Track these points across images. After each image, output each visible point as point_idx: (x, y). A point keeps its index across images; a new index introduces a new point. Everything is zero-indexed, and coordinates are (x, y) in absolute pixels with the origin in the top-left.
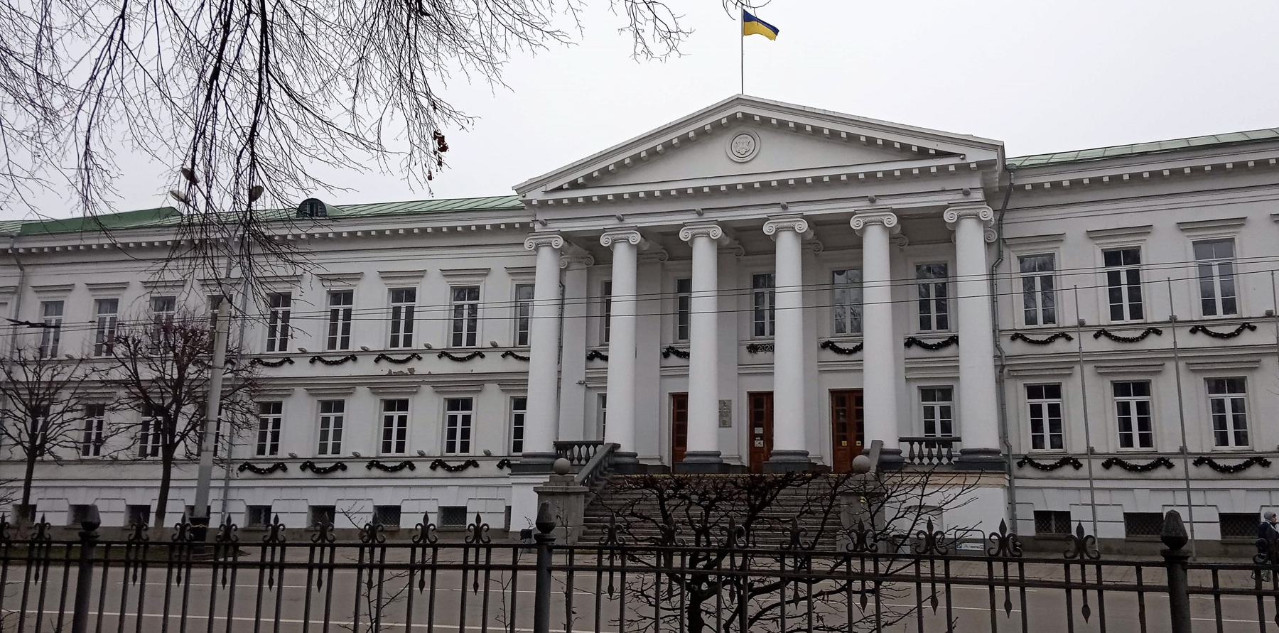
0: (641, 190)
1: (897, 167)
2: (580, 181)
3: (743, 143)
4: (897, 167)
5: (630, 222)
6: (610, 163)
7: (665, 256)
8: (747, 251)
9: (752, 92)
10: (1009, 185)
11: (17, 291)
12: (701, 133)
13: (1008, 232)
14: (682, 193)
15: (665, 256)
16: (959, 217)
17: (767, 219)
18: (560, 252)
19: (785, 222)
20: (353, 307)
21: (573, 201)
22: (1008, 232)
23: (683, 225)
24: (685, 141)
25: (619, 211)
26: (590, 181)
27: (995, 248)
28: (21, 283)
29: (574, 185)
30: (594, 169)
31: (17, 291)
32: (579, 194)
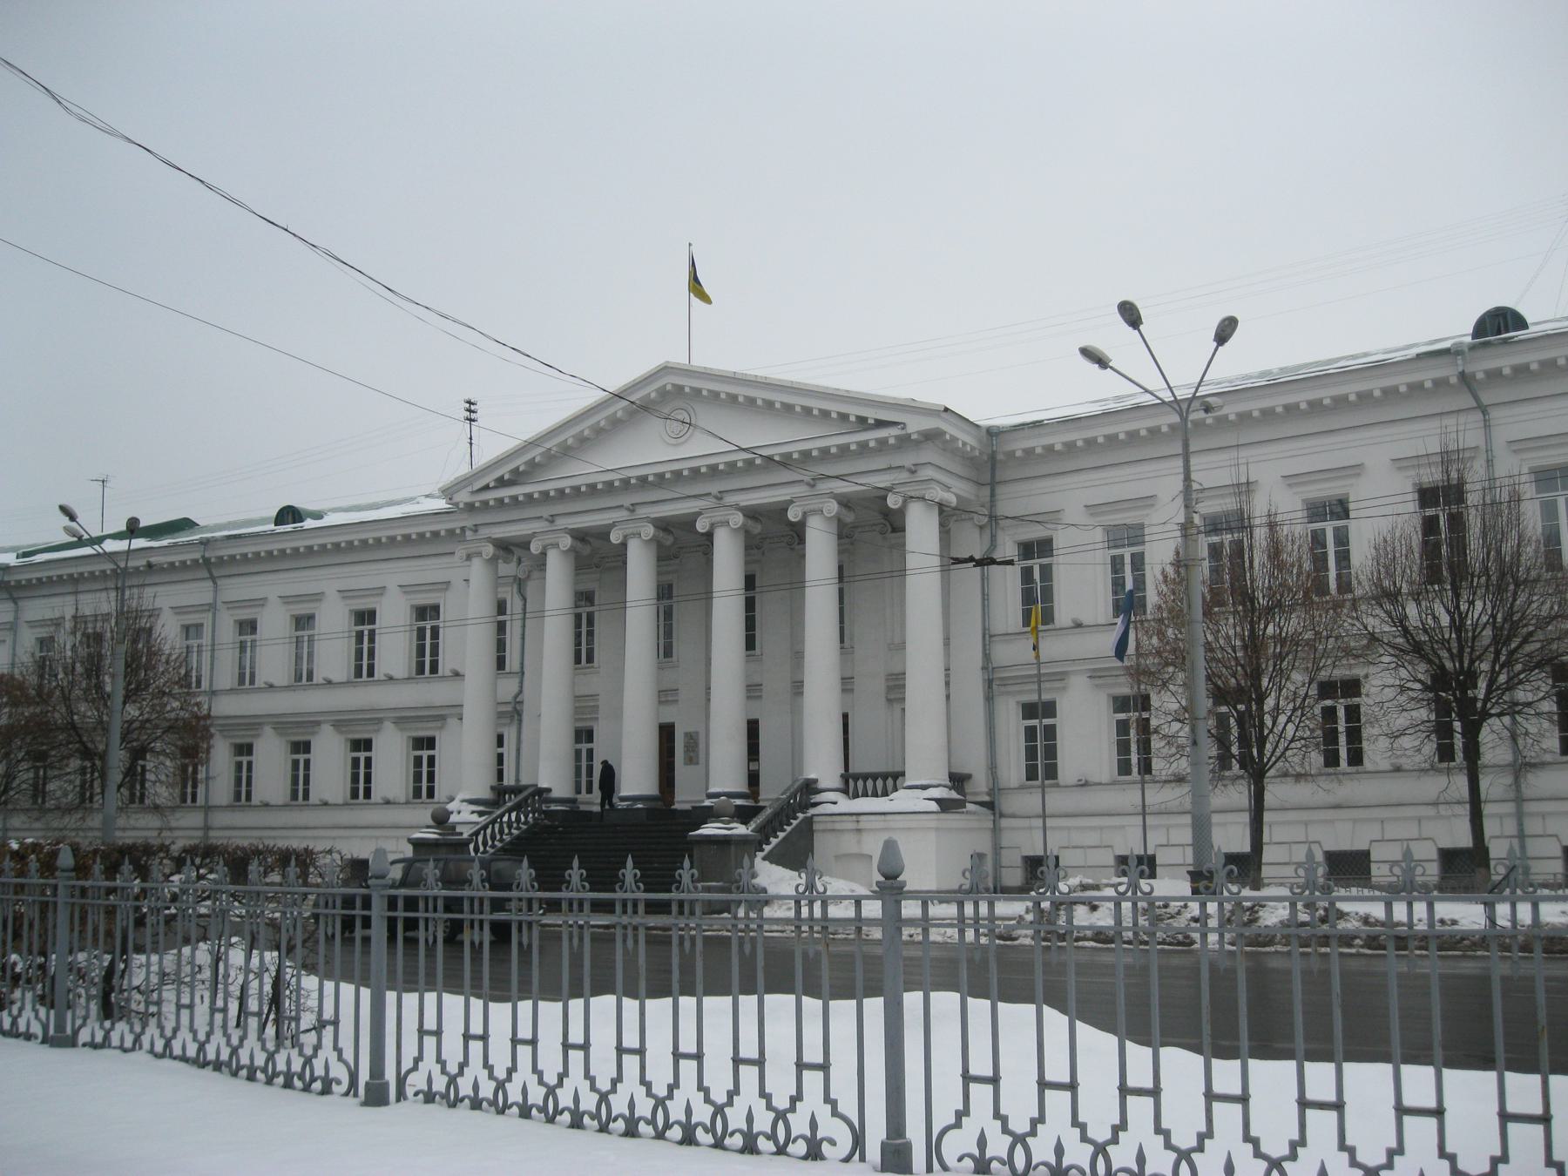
2: (506, 477)
4: (853, 439)
5: (562, 523)
7: (597, 559)
8: (682, 548)
9: (701, 361)
11: (13, 627)
15: (597, 559)
16: (805, 514)
17: (699, 514)
20: (376, 626)
21: (500, 501)
25: (546, 511)
27: (988, 531)
28: (16, 618)
30: (519, 462)
31: (13, 627)
32: (506, 493)
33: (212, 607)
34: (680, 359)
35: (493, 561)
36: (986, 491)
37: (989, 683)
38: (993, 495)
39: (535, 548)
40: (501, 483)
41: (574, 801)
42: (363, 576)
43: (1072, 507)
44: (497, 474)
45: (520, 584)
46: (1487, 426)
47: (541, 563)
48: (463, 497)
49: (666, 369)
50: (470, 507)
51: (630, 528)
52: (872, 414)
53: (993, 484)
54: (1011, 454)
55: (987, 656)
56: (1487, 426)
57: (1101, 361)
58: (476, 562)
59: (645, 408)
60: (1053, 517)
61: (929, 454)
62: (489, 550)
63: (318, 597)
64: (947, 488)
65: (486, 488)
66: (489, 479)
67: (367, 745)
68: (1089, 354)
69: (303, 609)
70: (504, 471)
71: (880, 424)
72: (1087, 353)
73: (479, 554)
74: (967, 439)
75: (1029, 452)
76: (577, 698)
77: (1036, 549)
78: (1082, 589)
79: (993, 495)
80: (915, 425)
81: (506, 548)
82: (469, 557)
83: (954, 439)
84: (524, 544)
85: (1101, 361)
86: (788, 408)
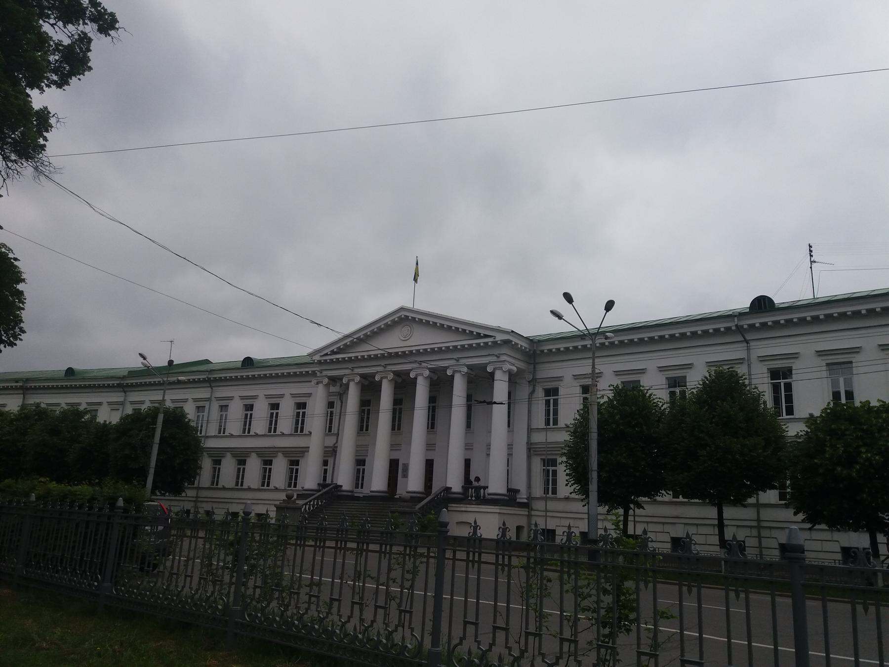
0: (359, 355)
3: (406, 330)
5: (357, 371)
10: (535, 352)
18: (327, 385)
23: (377, 372)
25: (350, 366)
26: (340, 351)
29: (333, 353)
30: (341, 344)
33: (209, 400)
35: (327, 385)
36: (532, 366)
37: (529, 449)
38: (535, 368)
39: (345, 381)
40: (333, 353)
41: (352, 492)
42: (275, 389)
43: (568, 375)
44: (331, 349)
47: (347, 385)
48: (317, 358)
49: (402, 309)
50: (319, 362)
54: (542, 351)
55: (529, 437)
57: (559, 317)
58: (321, 386)
60: (560, 379)
62: (326, 381)
63: (255, 397)
64: (513, 365)
65: (326, 354)
66: (328, 351)
68: (553, 313)
70: (334, 348)
72: (553, 313)
73: (322, 382)
75: (550, 350)
76: (357, 446)
77: (552, 392)
78: (569, 410)
79: (535, 368)
80: (500, 337)
81: (333, 380)
82: (318, 383)
83: (516, 344)
84: (340, 378)
85: (559, 317)
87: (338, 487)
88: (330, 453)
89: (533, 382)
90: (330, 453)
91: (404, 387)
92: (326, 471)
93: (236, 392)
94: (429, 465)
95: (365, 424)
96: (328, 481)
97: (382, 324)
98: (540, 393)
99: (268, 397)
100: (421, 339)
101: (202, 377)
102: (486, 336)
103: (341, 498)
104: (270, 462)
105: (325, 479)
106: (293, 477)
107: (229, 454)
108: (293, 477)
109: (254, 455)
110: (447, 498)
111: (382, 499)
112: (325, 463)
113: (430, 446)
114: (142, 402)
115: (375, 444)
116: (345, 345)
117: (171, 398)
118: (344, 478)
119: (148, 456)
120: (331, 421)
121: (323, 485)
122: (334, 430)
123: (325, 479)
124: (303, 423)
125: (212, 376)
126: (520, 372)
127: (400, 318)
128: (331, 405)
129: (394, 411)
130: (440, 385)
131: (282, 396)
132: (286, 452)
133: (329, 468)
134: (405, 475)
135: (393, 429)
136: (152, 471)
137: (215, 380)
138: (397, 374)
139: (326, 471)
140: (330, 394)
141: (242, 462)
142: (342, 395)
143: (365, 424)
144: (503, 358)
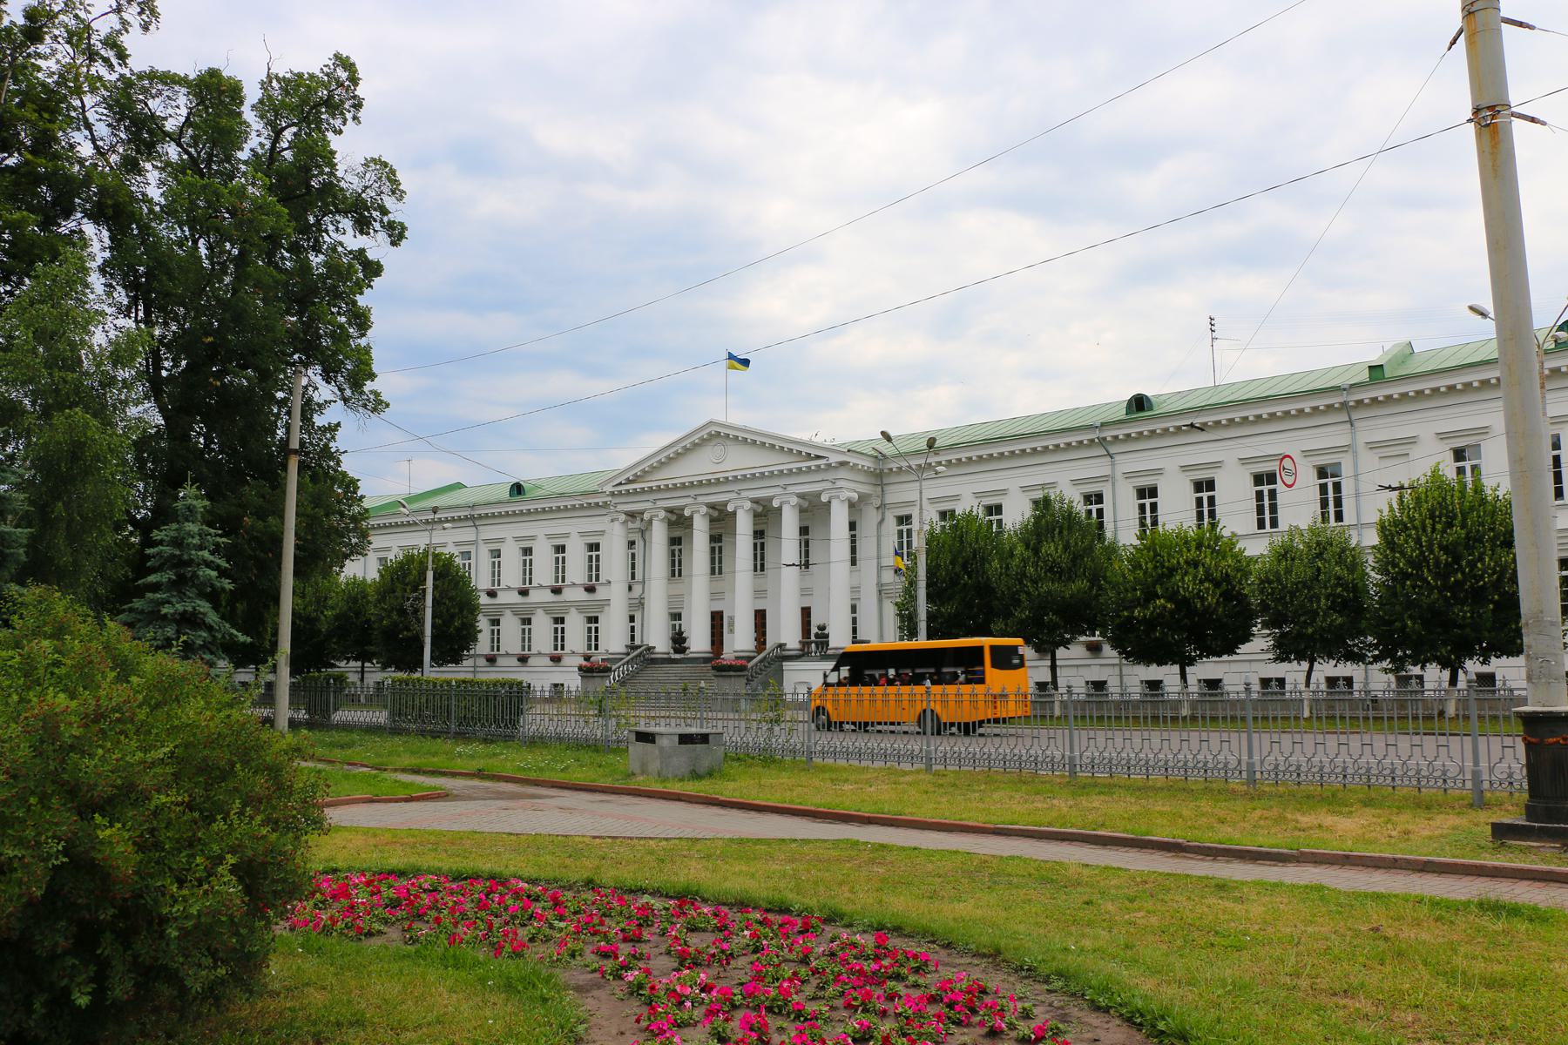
1: (804, 465)
4: (804, 465)
5: (660, 504)
6: (645, 466)
7: (679, 524)
12: (695, 446)
13: (889, 499)
14: (675, 487)
19: (739, 503)
22: (889, 499)
24: (686, 450)
25: (652, 497)
30: (637, 470)
32: (630, 487)
34: (721, 418)
35: (625, 522)
39: (646, 516)
40: (629, 481)
45: (643, 532)
46: (1113, 465)
47: (650, 522)
48: (608, 488)
50: (612, 494)
51: (695, 508)
52: (814, 452)
53: (882, 485)
55: (879, 576)
56: (1113, 465)
59: (703, 442)
61: (842, 473)
62: (623, 517)
66: (622, 479)
67: (562, 620)
69: (526, 544)
70: (630, 475)
71: (818, 457)
74: (867, 463)
76: (670, 596)
81: (632, 515)
84: (642, 513)
86: (773, 446)
87: (650, 649)
88: (636, 609)
89: (882, 507)
90: (636, 609)
91: (721, 520)
92: (633, 629)
93: (508, 535)
94: (760, 616)
95: (676, 568)
96: (638, 642)
97: (687, 443)
98: (891, 527)
99: (549, 537)
100: (738, 461)
101: (462, 514)
102: (818, 457)
103: (654, 661)
104: (529, 621)
105: (633, 638)
106: (593, 638)
107: (508, 612)
108: (593, 638)
109: (540, 612)
110: (783, 656)
111: (706, 660)
112: (632, 619)
113: (759, 593)
114: (388, 549)
115: (733, 591)
116: (643, 471)
117: (448, 541)
118: (658, 639)
119: (421, 622)
120: (633, 567)
121: (633, 648)
122: (639, 576)
123: (633, 638)
124: (598, 569)
125: (476, 513)
126: (863, 498)
127: (710, 434)
128: (632, 544)
129: (713, 550)
130: (765, 517)
131: (567, 535)
132: (580, 607)
133: (637, 624)
134: (731, 631)
135: (713, 572)
136: (428, 641)
137: (480, 517)
138: (712, 506)
139: (633, 629)
140: (630, 531)
141: (527, 621)
142: (644, 532)
143: (676, 568)
144: (839, 484)
